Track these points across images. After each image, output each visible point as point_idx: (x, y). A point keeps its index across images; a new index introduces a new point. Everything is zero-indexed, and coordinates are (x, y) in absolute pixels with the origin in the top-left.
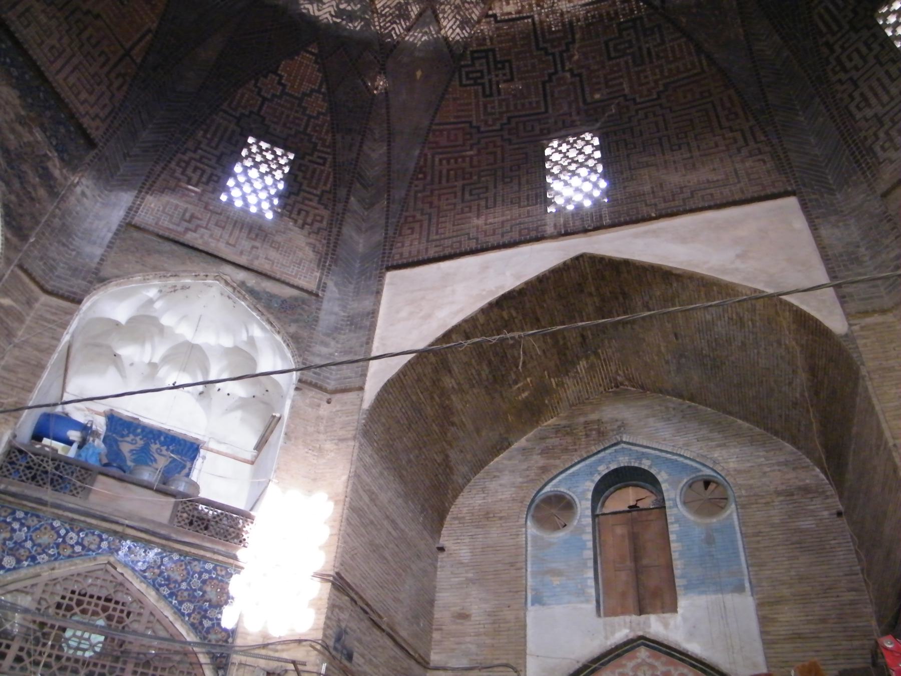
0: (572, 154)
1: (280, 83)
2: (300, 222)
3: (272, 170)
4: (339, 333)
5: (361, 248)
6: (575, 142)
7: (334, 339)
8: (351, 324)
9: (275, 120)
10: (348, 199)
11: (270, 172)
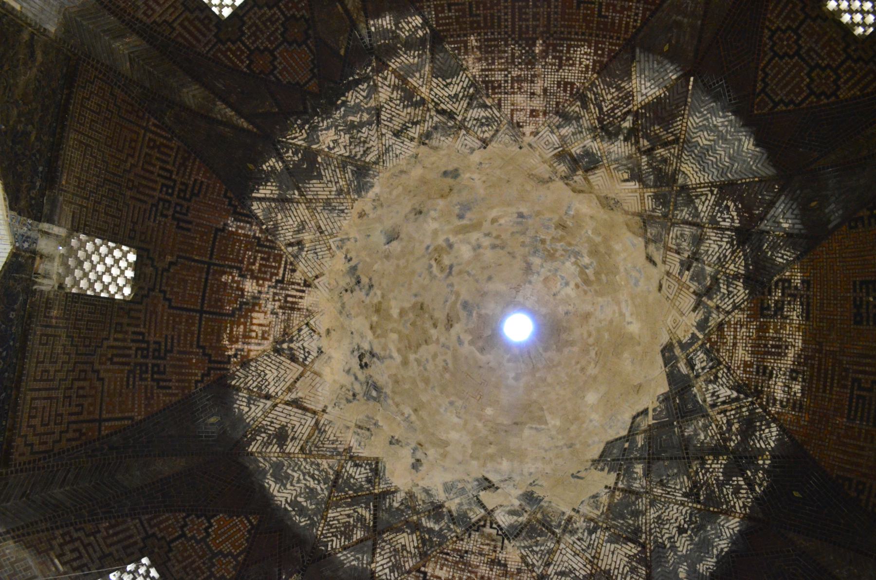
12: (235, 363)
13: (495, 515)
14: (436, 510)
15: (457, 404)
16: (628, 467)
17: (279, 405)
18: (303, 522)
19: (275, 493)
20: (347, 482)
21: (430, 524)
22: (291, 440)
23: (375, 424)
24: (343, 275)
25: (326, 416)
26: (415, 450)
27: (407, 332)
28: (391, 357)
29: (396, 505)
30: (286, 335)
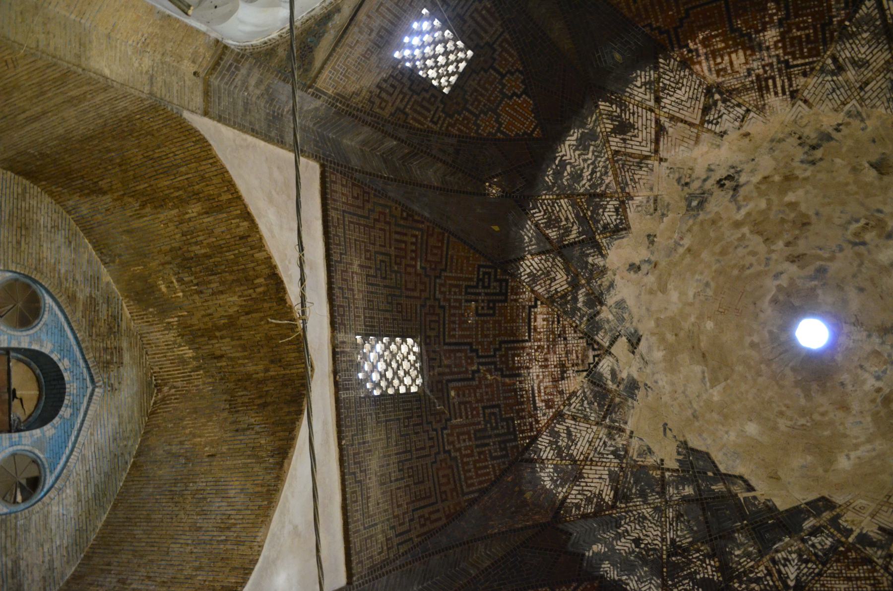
0: (406, 365)
1: (514, 94)
2: (384, 85)
3: (438, 68)
4: (267, 102)
5: (346, 142)
6: (416, 368)
7: (262, 95)
8: (274, 117)
9: (482, 82)
10: (396, 138)
11: (436, 66)
12: (682, 54)
13: (607, 357)
14: (596, 300)
15: (708, 290)
16: (687, 479)
17: (653, 114)
18: (549, 179)
19: (567, 143)
20: (598, 206)
21: (581, 298)
22: (622, 139)
23: (663, 215)
24: (817, 129)
25: (656, 163)
26: (649, 261)
27: (772, 217)
28: (739, 209)
29: (590, 260)
30: (728, 94)
